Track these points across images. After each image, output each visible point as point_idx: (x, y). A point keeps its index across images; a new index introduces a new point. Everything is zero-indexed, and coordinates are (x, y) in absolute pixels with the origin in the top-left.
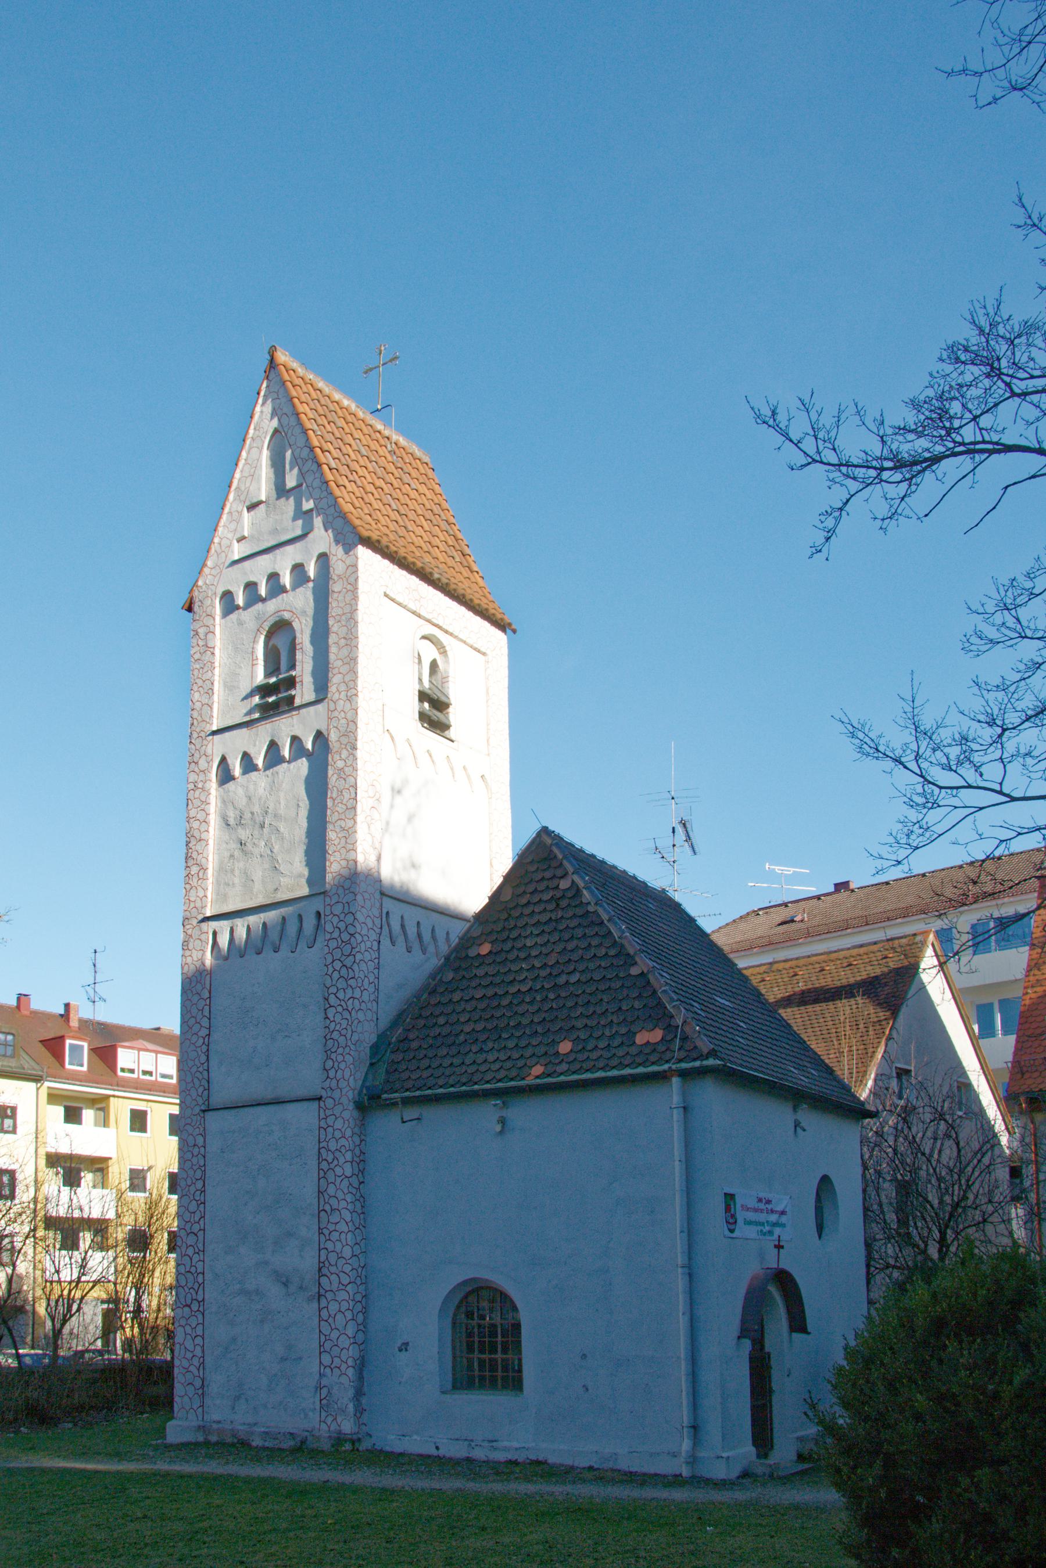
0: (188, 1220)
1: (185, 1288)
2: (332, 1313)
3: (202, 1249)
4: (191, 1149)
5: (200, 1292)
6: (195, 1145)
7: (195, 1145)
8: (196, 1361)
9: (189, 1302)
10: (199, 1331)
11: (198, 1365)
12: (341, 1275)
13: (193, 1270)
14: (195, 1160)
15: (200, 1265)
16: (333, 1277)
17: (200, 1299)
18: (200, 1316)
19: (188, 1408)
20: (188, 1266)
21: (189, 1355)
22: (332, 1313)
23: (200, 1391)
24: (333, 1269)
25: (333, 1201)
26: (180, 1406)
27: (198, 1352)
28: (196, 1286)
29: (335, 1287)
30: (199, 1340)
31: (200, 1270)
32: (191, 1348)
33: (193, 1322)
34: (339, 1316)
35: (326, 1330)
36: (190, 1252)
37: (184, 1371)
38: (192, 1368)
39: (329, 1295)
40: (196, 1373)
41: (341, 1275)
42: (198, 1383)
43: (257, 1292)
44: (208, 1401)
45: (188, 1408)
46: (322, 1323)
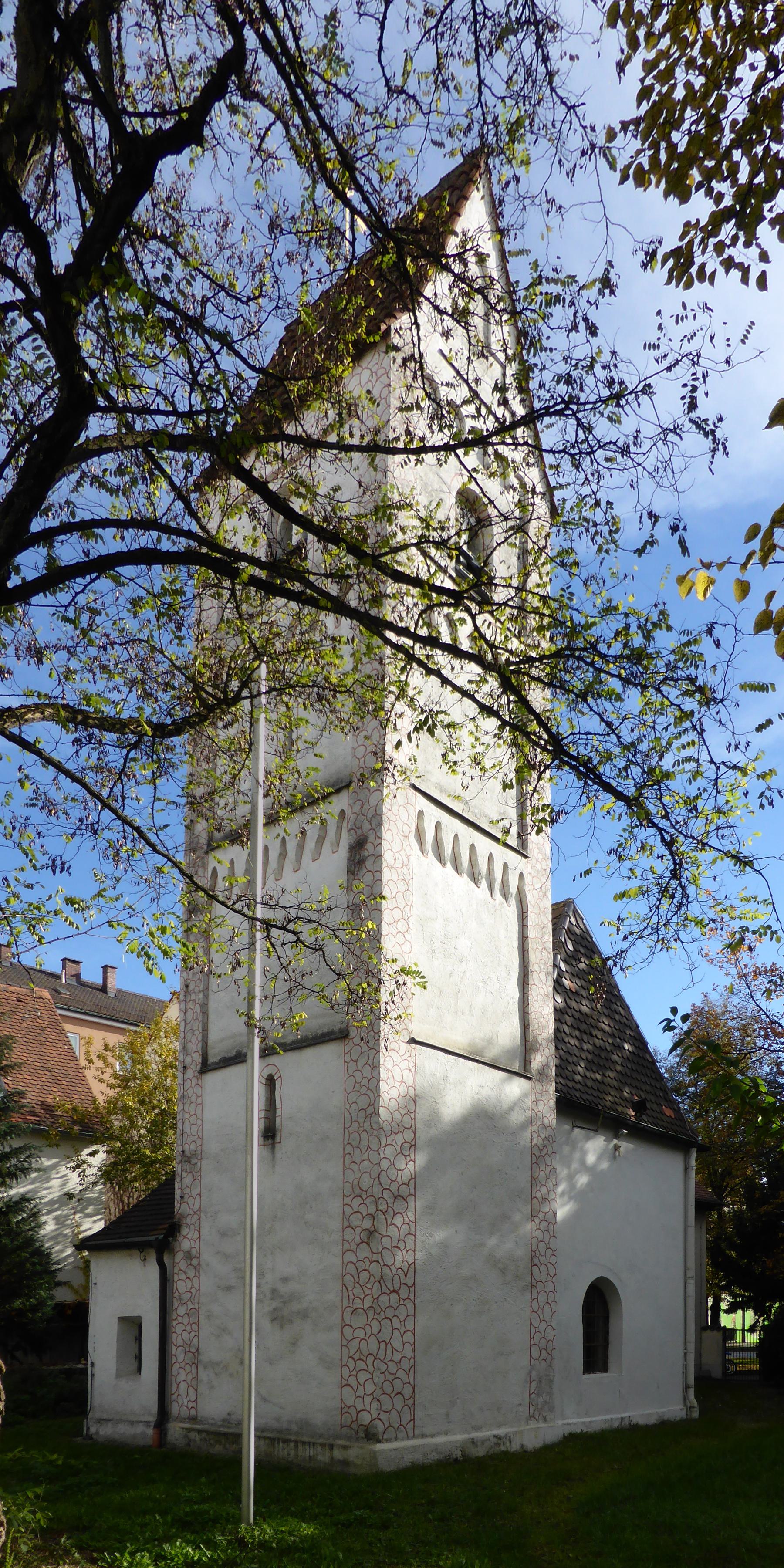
1: (393, 1268)
2: (541, 1304)
3: (412, 1219)
8: (405, 1365)
9: (397, 1287)
11: (407, 1368)
16: (543, 1268)
17: (410, 1283)
18: (410, 1306)
19: (396, 1425)
21: (397, 1357)
22: (541, 1304)
23: (410, 1402)
24: (542, 1259)
26: (387, 1424)
27: (408, 1352)
29: (543, 1278)
34: (547, 1308)
37: (391, 1378)
38: (400, 1374)
39: (539, 1285)
40: (406, 1380)
42: (407, 1392)
44: (419, 1414)
45: (396, 1425)
46: (534, 1315)
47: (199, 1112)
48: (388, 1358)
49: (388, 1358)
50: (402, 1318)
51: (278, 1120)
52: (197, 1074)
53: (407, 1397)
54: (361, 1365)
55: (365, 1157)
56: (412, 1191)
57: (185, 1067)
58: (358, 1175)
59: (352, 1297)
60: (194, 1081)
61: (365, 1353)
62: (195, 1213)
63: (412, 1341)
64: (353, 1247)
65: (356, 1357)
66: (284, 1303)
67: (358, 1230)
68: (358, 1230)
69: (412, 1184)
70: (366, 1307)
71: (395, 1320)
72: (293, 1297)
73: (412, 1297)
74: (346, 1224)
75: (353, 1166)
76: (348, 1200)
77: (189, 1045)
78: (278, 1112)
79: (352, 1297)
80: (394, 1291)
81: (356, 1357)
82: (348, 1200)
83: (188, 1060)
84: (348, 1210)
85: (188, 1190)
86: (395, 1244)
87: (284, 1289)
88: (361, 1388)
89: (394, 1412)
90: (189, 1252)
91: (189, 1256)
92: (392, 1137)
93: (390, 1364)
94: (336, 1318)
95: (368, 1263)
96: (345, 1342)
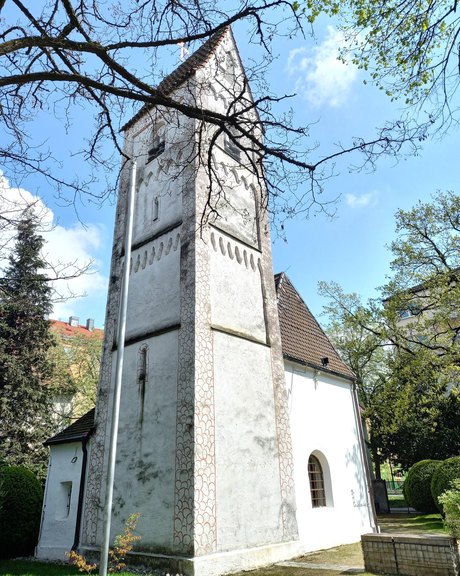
0: (202, 396)
1: (202, 445)
3: (213, 418)
4: (204, 349)
5: (212, 449)
6: (206, 348)
7: (206, 348)
8: (210, 505)
9: (205, 457)
10: (212, 479)
11: (211, 506)
12: (287, 443)
13: (207, 432)
14: (206, 357)
15: (211, 429)
16: (284, 444)
20: (204, 429)
21: (205, 499)
23: (214, 528)
25: (281, 401)
27: (212, 496)
28: (209, 445)
29: (285, 450)
30: (212, 487)
31: (212, 433)
32: (206, 493)
33: (208, 472)
35: (283, 477)
36: (205, 419)
41: (287, 443)
42: (212, 521)
43: (248, 450)
44: (219, 536)
47: (110, 370)
48: (200, 500)
49: (200, 500)
50: (208, 475)
51: (147, 370)
52: (110, 352)
53: (212, 525)
54: (185, 505)
55: (188, 385)
56: (213, 403)
57: (105, 349)
58: (184, 395)
59: (181, 463)
60: (109, 355)
61: (188, 498)
62: (104, 421)
63: (214, 489)
64: (182, 435)
65: (183, 500)
66: (146, 469)
67: (184, 425)
68: (184, 425)
69: (212, 399)
70: (188, 469)
71: (204, 476)
72: (150, 465)
73: (213, 463)
74: (178, 422)
75: (183, 391)
76: (179, 409)
77: (108, 338)
78: (147, 366)
79: (181, 463)
80: (203, 459)
81: (183, 500)
82: (179, 409)
83: (107, 345)
84: (179, 414)
85: (101, 410)
86: (203, 432)
87: (146, 461)
88: (185, 520)
89: (204, 535)
90: (99, 443)
91: (99, 445)
92: (202, 375)
93: (201, 504)
94: (171, 477)
95: (189, 443)
96: (177, 491)
